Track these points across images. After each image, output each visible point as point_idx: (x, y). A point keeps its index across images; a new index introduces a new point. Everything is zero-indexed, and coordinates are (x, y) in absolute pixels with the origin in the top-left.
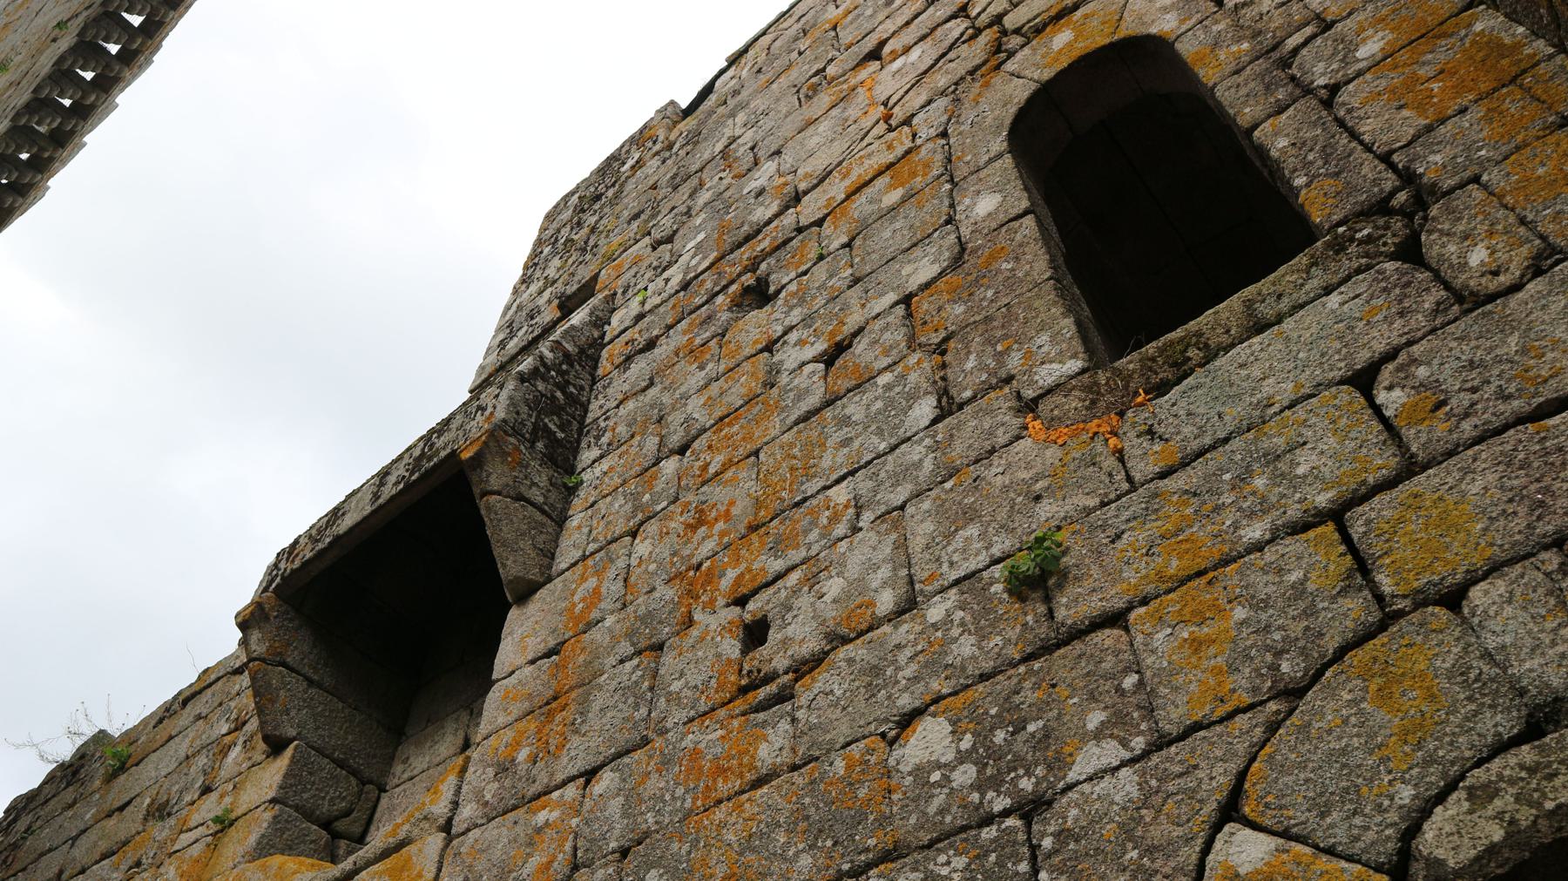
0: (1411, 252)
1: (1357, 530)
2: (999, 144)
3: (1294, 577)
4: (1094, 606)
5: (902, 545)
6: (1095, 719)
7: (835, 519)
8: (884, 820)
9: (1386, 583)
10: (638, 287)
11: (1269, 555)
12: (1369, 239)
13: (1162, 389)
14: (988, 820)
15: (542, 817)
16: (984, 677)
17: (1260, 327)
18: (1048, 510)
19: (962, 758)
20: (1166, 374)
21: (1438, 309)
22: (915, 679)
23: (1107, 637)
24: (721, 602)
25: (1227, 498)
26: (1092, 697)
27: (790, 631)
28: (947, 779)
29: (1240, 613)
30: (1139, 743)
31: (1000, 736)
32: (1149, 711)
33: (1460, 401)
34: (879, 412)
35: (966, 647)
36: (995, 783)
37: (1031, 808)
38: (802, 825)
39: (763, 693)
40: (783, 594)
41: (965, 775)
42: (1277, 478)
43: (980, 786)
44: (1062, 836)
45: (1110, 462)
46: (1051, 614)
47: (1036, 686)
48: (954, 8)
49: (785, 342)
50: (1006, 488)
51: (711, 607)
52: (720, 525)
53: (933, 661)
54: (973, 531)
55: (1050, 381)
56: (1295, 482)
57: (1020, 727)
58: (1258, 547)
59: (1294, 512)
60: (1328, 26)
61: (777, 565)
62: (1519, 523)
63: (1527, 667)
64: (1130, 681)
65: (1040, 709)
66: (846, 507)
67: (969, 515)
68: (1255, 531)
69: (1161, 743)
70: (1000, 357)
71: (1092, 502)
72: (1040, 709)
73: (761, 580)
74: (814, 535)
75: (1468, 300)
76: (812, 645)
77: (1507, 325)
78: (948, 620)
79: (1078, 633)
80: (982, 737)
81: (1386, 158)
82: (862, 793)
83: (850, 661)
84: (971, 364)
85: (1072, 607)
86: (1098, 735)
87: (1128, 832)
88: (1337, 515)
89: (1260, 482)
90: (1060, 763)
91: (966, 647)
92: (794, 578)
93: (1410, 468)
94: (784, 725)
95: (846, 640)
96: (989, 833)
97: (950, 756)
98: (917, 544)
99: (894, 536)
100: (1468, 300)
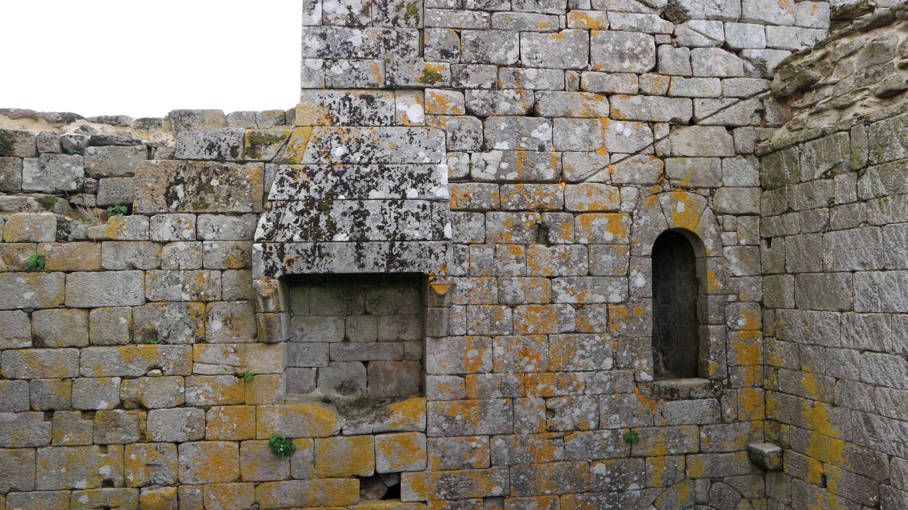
0: (719, 398)
1: (688, 460)
2: (648, 249)
3: (676, 465)
4: (640, 452)
5: (598, 409)
6: (636, 479)
7: (578, 386)
8: (588, 484)
9: (688, 474)
10: (465, 147)
11: (674, 458)
12: (716, 390)
13: (667, 400)
14: (611, 491)
15: (474, 444)
16: (615, 458)
17: (690, 398)
18: (635, 420)
19: (608, 476)
20: (669, 397)
21: (717, 420)
22: (598, 451)
23: (641, 460)
24: (538, 395)
25: (671, 441)
26: (636, 473)
27: (564, 419)
28: (603, 480)
29: (665, 468)
30: (642, 487)
31: (616, 474)
32: (645, 480)
33: (711, 443)
34: (595, 352)
35: (611, 449)
36: (614, 484)
37: (619, 491)
38: (567, 478)
39: (554, 434)
40: (561, 405)
41: (608, 480)
42: (681, 441)
43: (611, 483)
44: (625, 499)
45: (651, 416)
46: (631, 449)
47: (625, 466)
48: (650, 119)
49: (559, 282)
50: (628, 408)
51: (533, 393)
52: (534, 361)
53: (603, 449)
54: (617, 416)
55: (644, 379)
56: (683, 445)
57: (621, 473)
58: (671, 455)
59: (680, 452)
60: (738, 300)
61: (558, 392)
62: (708, 473)
63: (699, 496)
64: (643, 473)
65: (625, 472)
66: (582, 384)
67: (617, 411)
68: (673, 451)
69: (646, 488)
70: (633, 358)
71: (646, 425)
72: (625, 472)
73: (552, 395)
74: (571, 388)
75: (722, 421)
76: (570, 428)
77: (725, 432)
78: (607, 439)
79: (636, 457)
80: (613, 472)
81: (728, 366)
82: (584, 475)
83: (582, 438)
84: (625, 354)
85: (637, 450)
86: (635, 482)
87: (637, 502)
88: (686, 454)
89: (677, 440)
90: (627, 485)
91: (611, 449)
92: (564, 401)
93: (700, 452)
94: (562, 448)
95: (579, 430)
96: (611, 494)
97: (604, 474)
98: (603, 412)
99: (596, 405)
100: (722, 421)
